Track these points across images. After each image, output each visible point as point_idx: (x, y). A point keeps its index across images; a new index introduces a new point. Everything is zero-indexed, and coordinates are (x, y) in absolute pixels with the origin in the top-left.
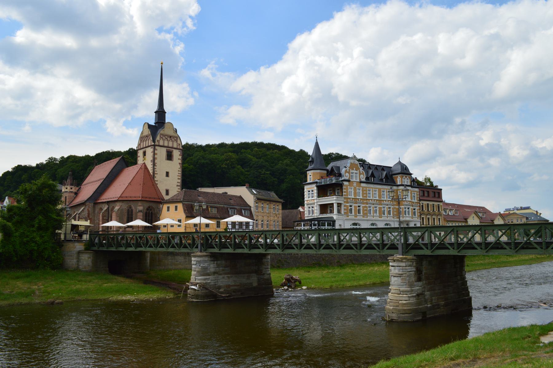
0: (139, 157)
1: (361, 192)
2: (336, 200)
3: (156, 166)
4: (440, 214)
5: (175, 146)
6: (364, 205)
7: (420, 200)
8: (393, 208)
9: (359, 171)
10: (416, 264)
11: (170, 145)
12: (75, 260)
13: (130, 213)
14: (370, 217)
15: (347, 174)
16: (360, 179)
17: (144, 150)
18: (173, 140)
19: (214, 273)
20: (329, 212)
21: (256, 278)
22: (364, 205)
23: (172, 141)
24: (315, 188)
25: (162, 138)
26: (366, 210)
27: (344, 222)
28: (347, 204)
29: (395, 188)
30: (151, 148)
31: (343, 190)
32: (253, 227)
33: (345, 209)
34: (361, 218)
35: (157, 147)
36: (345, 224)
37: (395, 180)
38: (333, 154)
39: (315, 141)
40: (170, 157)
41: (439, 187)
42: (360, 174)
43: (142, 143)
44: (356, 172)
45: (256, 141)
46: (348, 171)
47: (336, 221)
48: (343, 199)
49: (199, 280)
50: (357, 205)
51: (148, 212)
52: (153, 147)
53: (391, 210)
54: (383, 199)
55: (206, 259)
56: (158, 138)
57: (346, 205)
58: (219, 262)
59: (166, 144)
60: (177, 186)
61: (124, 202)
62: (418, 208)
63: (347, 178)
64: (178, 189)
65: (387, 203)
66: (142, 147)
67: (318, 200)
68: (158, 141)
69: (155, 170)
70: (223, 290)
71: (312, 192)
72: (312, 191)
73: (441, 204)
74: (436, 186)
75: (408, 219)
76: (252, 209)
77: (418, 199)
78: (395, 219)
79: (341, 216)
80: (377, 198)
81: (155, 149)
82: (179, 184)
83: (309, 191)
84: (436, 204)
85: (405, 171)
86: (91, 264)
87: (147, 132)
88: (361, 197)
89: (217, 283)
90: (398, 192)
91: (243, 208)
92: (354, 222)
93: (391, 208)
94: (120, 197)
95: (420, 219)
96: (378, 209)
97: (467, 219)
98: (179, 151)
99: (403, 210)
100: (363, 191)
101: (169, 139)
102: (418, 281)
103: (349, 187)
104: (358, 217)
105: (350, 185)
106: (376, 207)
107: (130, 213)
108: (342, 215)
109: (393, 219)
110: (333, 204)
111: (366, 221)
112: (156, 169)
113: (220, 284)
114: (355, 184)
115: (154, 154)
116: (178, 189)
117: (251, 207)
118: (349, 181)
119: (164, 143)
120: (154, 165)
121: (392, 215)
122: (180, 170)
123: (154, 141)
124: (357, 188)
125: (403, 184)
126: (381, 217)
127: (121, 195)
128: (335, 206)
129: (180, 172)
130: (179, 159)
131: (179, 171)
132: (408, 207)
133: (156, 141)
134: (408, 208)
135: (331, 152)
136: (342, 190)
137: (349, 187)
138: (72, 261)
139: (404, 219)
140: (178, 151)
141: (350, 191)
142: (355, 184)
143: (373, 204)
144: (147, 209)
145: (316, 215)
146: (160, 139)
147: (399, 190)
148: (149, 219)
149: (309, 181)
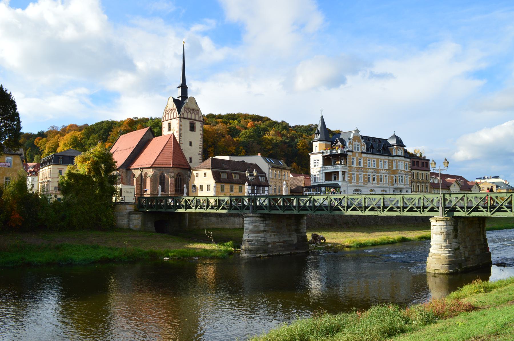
0: (164, 128)
1: (362, 162)
2: (341, 168)
3: (181, 136)
4: (427, 182)
5: (197, 118)
6: (364, 174)
7: (412, 169)
8: (388, 176)
9: (361, 143)
10: (454, 224)
11: (193, 117)
12: (126, 220)
13: (162, 179)
14: (370, 184)
15: (351, 145)
16: (361, 150)
17: (169, 121)
18: (195, 112)
19: (264, 231)
20: (333, 179)
21: (296, 236)
22: (364, 174)
23: (194, 114)
24: (321, 158)
25: (186, 111)
26: (366, 178)
27: (348, 188)
28: (350, 173)
29: (391, 158)
30: (176, 120)
31: (347, 160)
33: (348, 177)
34: (362, 184)
35: (182, 120)
36: (349, 190)
37: (390, 151)
38: (312, 125)
39: (321, 116)
40: (192, 128)
41: (427, 158)
42: (362, 145)
43: (167, 116)
44: (358, 143)
45: (241, 113)
46: (351, 142)
47: (341, 187)
48: (347, 168)
49: (252, 237)
50: (379, 174)
51: (177, 177)
52: (179, 119)
53: (387, 178)
54: (369, 167)
55: (258, 219)
56: (182, 110)
57: (349, 173)
58: (267, 222)
59: (189, 117)
60: (199, 154)
61: (157, 168)
62: (409, 176)
63: (351, 149)
64: (200, 157)
65: (384, 171)
66: (167, 119)
67: (323, 169)
68: (182, 113)
70: (271, 246)
71: (318, 161)
72: (318, 160)
73: (429, 173)
75: (401, 186)
76: (267, 176)
77: (410, 168)
78: (390, 186)
79: (345, 183)
80: (376, 167)
81: (180, 121)
82: (200, 153)
83: (315, 161)
84: (424, 172)
85: (400, 143)
86: (140, 224)
87: (172, 105)
88: (362, 166)
89: (266, 240)
90: (393, 162)
91: (260, 175)
92: (356, 188)
93: (387, 177)
94: (153, 164)
95: (411, 186)
96: (376, 177)
97: (450, 186)
98: (200, 123)
99: (397, 178)
100: (364, 160)
101: (192, 112)
102: (455, 238)
103: (352, 157)
104: (360, 184)
105: (353, 155)
106: (374, 175)
107: (162, 179)
108: (346, 182)
109: (389, 186)
110: (338, 172)
111: (366, 188)
112: (181, 139)
113: (268, 240)
114: (357, 155)
115: (180, 126)
116: (200, 157)
117: (266, 174)
118: (352, 151)
119: (195, 117)
120: (180, 135)
121: (387, 182)
122: (201, 140)
123: (179, 112)
124: (359, 158)
125: (398, 155)
126: (378, 184)
127: (154, 162)
128: (340, 173)
129: (201, 142)
131: (200, 141)
132: (402, 175)
133: (181, 113)
134: (402, 177)
135: (311, 123)
136: (346, 160)
137: (352, 157)
138: (124, 220)
139: (399, 186)
140: (199, 122)
142: (357, 155)
143: (372, 173)
144: (177, 175)
145: (321, 181)
146: (185, 112)
147: (394, 160)
148: (178, 184)
149: (314, 151)
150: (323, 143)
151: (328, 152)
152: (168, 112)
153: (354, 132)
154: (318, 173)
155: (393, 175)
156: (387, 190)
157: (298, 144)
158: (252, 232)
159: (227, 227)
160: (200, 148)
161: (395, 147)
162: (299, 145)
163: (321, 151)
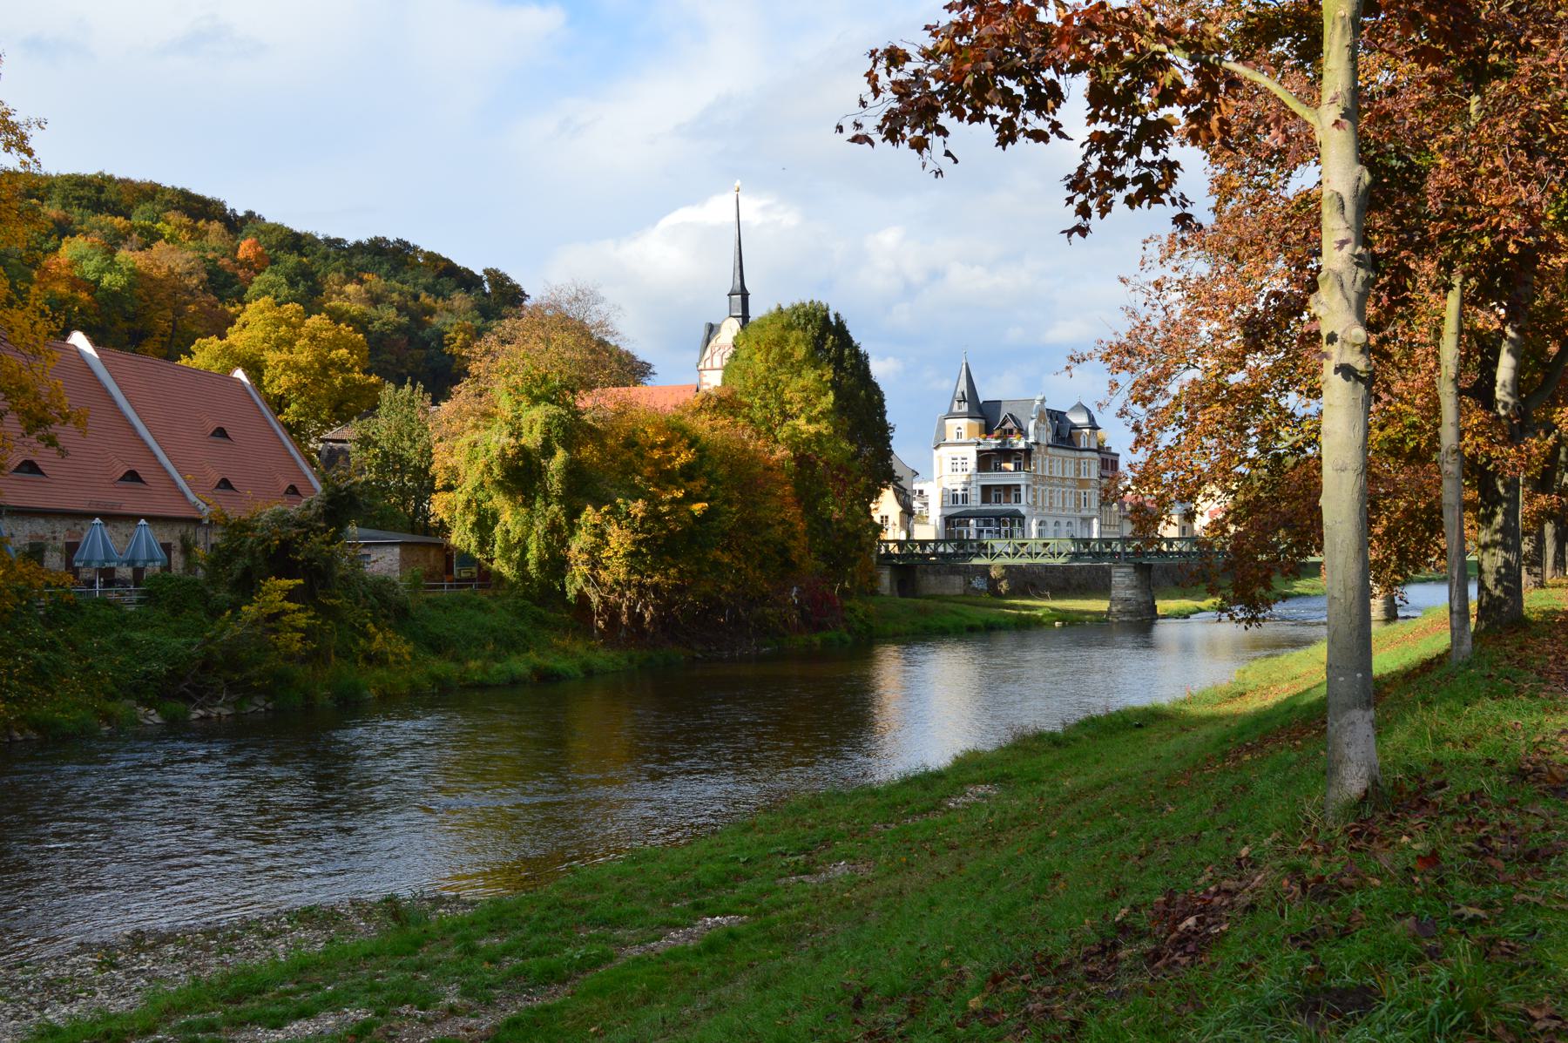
7: (1102, 477)
20: (993, 499)
29: (1078, 454)
41: (1113, 451)
74: (1109, 448)
110: (1018, 487)
141: (1040, 464)
150: (975, 423)
151: (993, 443)
152: (722, 351)
153: (1038, 403)
154: (962, 486)
155: (1082, 491)
156: (1073, 520)
157: (451, 338)
158: (1128, 587)
159: (947, 592)
161: (1087, 431)
162: (454, 340)
163: (972, 440)
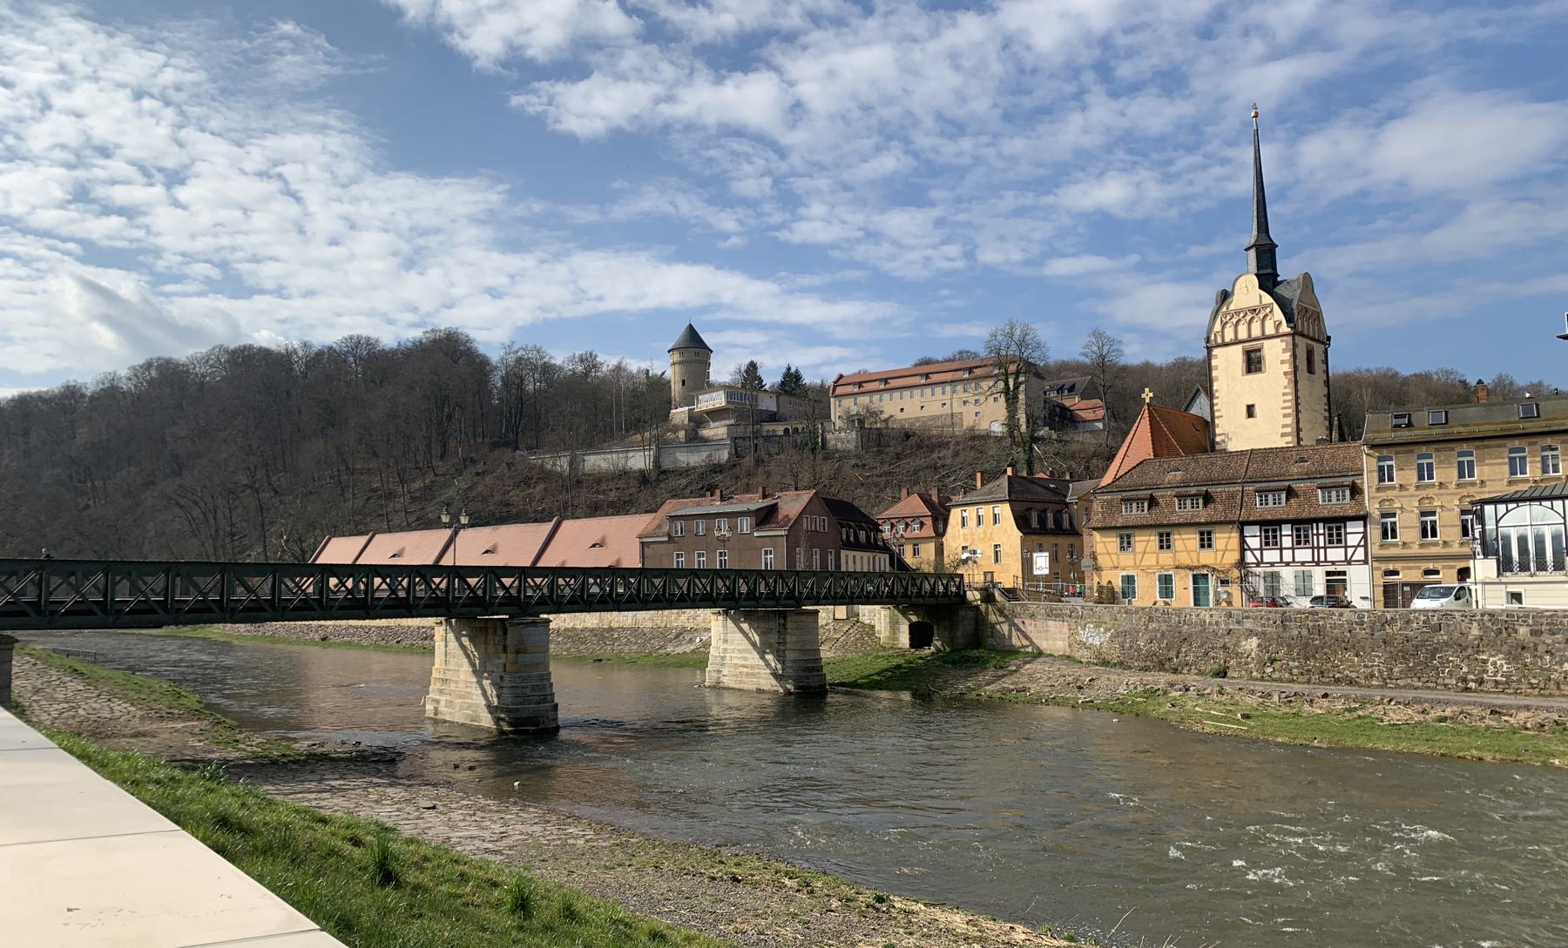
5: (1270, 330)
32: (1365, 537)
59: (1243, 335)
69: (1215, 408)
82: (1289, 430)
130: (1283, 362)
131: (1284, 394)
140: (1279, 340)
160: (1285, 416)
